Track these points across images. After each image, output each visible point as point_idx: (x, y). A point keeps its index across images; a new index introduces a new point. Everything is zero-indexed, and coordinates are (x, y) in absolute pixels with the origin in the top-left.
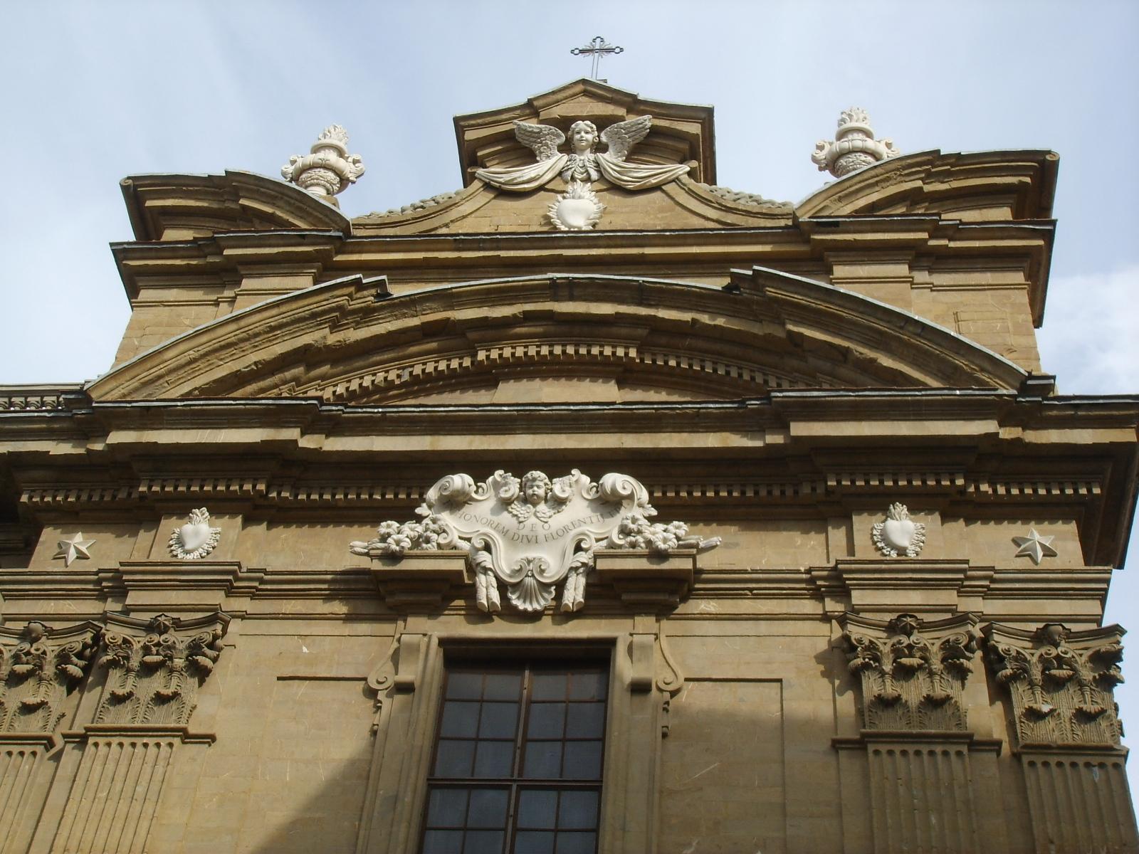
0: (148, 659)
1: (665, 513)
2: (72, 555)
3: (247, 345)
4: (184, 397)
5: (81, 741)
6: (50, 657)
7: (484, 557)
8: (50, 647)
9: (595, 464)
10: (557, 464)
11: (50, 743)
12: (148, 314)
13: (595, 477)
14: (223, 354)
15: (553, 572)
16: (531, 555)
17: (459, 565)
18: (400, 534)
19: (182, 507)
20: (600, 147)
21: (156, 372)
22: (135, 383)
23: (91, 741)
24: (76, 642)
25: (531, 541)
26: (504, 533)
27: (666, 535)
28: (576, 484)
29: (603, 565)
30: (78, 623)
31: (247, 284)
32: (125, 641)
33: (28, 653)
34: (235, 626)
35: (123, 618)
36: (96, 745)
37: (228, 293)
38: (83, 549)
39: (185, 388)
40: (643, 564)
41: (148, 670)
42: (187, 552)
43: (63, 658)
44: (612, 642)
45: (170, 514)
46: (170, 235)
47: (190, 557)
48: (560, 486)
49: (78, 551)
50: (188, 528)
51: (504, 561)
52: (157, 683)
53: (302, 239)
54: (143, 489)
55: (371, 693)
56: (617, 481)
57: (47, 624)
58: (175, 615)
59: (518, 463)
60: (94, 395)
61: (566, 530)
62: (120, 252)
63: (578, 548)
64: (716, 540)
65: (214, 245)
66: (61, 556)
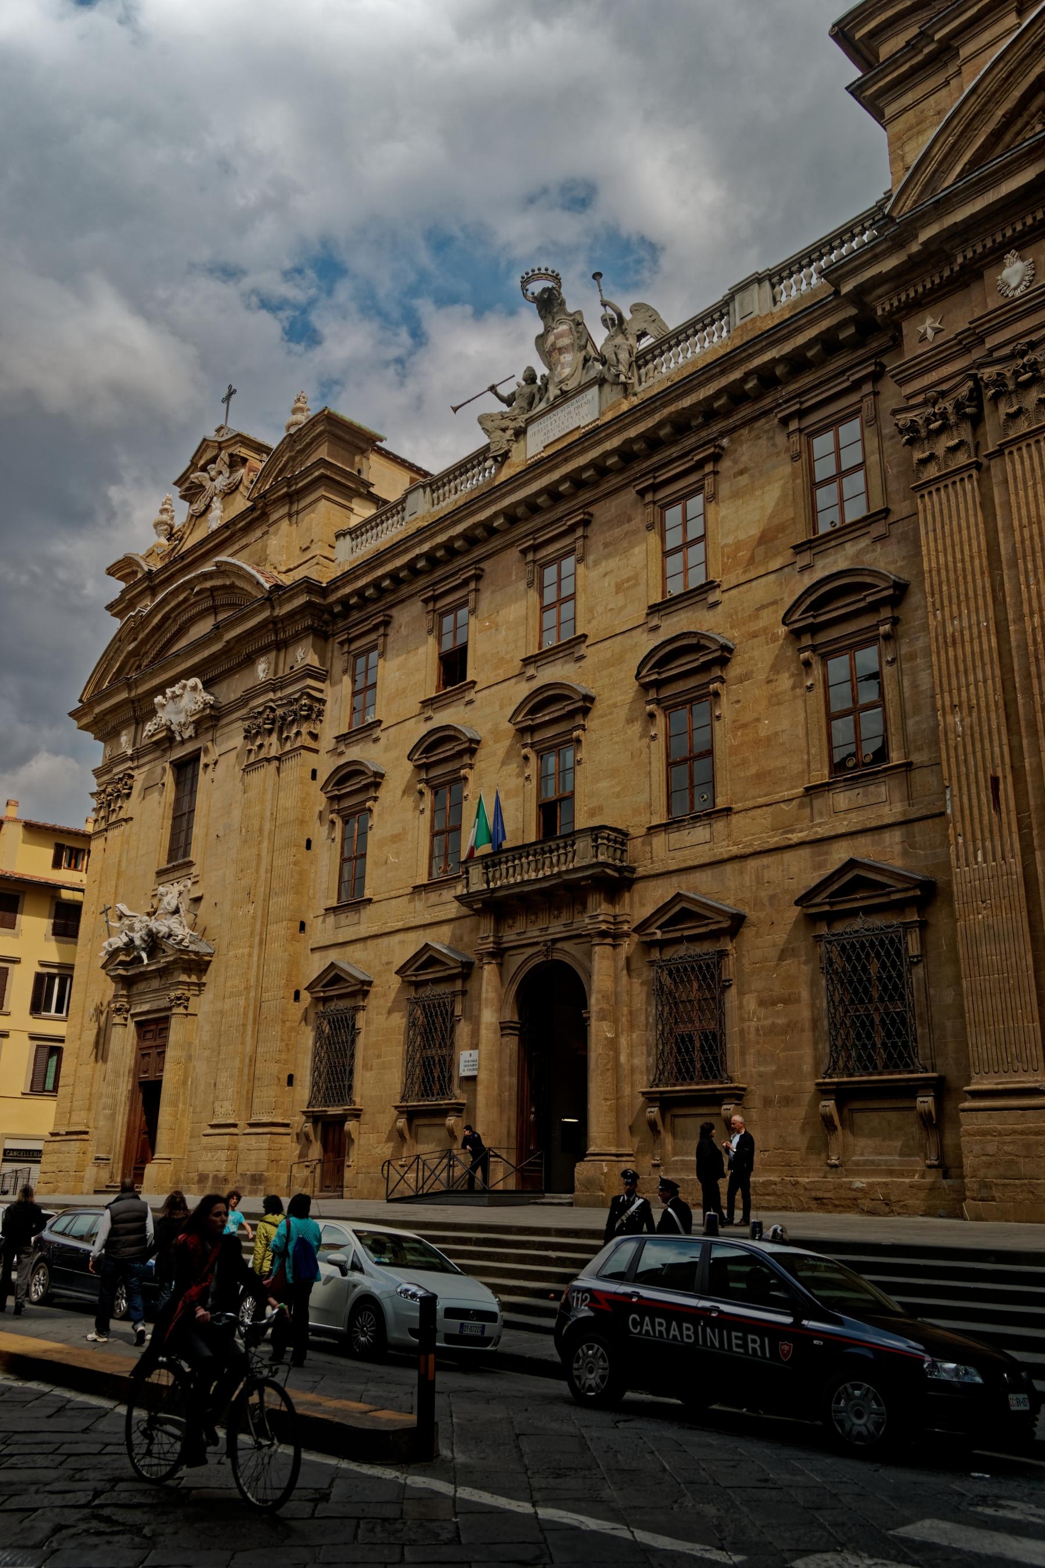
0: (1022, 378)
2: (930, 333)
3: (991, 105)
4: (960, 177)
5: (999, 452)
6: (950, 409)
8: (948, 405)
11: (978, 466)
12: (899, 125)
14: (975, 124)
19: (996, 257)
21: (930, 170)
22: (918, 189)
23: (1006, 452)
24: (964, 391)
30: (958, 379)
31: (965, 52)
32: (999, 374)
33: (935, 414)
35: (989, 359)
36: (1011, 453)
37: (952, 69)
38: (937, 325)
39: (958, 169)
42: (1015, 289)
43: (959, 406)
45: (989, 265)
46: (887, 49)
47: (1018, 293)
49: (933, 329)
50: (1006, 272)
54: (960, 260)
57: (938, 389)
58: (1027, 339)
60: (894, 214)
62: (855, 90)
65: (924, 36)
66: (923, 338)
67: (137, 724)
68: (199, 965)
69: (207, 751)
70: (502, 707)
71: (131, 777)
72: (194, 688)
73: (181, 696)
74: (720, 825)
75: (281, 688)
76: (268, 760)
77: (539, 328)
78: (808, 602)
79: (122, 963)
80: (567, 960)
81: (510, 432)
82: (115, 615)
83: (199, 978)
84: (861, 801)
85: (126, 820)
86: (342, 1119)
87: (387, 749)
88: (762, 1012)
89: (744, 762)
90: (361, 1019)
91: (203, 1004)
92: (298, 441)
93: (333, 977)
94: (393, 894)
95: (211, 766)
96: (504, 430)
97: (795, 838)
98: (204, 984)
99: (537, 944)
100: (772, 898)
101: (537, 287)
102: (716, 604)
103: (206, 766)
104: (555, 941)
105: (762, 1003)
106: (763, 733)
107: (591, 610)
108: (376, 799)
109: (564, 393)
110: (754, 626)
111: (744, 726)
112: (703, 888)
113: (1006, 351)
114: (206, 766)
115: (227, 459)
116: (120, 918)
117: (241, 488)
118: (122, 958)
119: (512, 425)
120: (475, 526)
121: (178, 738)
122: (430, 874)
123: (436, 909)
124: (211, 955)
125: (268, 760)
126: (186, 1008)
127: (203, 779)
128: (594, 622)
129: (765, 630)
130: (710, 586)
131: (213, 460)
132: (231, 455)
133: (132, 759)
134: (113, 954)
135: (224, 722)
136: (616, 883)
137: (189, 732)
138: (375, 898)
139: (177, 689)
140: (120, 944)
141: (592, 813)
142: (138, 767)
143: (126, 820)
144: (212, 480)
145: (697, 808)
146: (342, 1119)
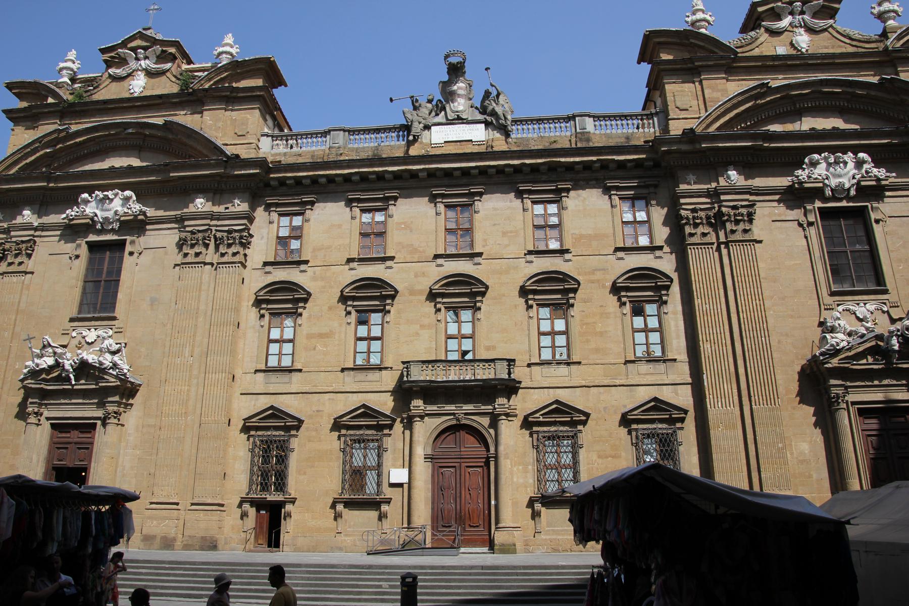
1: (877, 166)
7: (826, 181)
9: (855, 150)
10: (844, 150)
13: (855, 154)
15: (847, 186)
16: (841, 180)
17: (821, 185)
18: (802, 174)
20: (802, 13)
24: (711, 213)
25: (840, 176)
26: (831, 173)
27: (881, 173)
28: (849, 157)
29: (863, 183)
34: (758, 204)
40: (874, 183)
41: (737, 222)
43: (708, 217)
44: (867, 206)
48: (846, 157)
50: (729, 172)
51: (833, 182)
52: (741, 226)
53: (722, 58)
55: (800, 225)
56: (861, 155)
59: (833, 150)
61: (849, 172)
63: (854, 178)
64: (894, 174)
65: (691, 60)
67: (41, 205)
68: (128, 390)
69: (132, 242)
70: (416, 276)
71: (35, 242)
72: (127, 199)
73: (111, 200)
74: (573, 367)
75: (218, 219)
76: (205, 264)
77: (446, 78)
78: (627, 276)
79: (44, 380)
80: (475, 425)
81: (422, 125)
82: (11, 119)
83: (128, 400)
84: (652, 371)
85: (26, 273)
86: (279, 505)
87: (314, 278)
88: (600, 461)
89: (588, 341)
90: (294, 443)
91: (132, 418)
92: (239, 68)
93: (275, 413)
94: (323, 369)
95: (136, 255)
96: (420, 123)
97: (618, 382)
98: (132, 405)
99: (454, 414)
100: (605, 408)
101: (454, 60)
102: (569, 260)
103: (131, 254)
104: (466, 414)
105: (599, 457)
106: (598, 330)
107: (485, 240)
108: (305, 308)
109: (459, 118)
110: (593, 277)
111: (587, 324)
112: (565, 396)
113: (731, 204)
114: (131, 254)
115: (158, 53)
116: (44, 347)
117: (168, 74)
118: (44, 376)
119: (423, 121)
120: (406, 170)
121: (99, 226)
122: (355, 362)
123: (363, 384)
124: (140, 385)
125: (205, 264)
126: (119, 420)
127: (128, 261)
128: (487, 248)
129: (598, 281)
130: (567, 251)
131: (145, 48)
132: (163, 52)
133: (36, 229)
134: (34, 374)
135: (148, 227)
136: (510, 388)
137: (116, 226)
138: (304, 370)
139: (110, 194)
140: (45, 366)
141: (488, 349)
142: (41, 236)
143: (26, 273)
144: (137, 59)
145: (557, 357)
146: (279, 505)
